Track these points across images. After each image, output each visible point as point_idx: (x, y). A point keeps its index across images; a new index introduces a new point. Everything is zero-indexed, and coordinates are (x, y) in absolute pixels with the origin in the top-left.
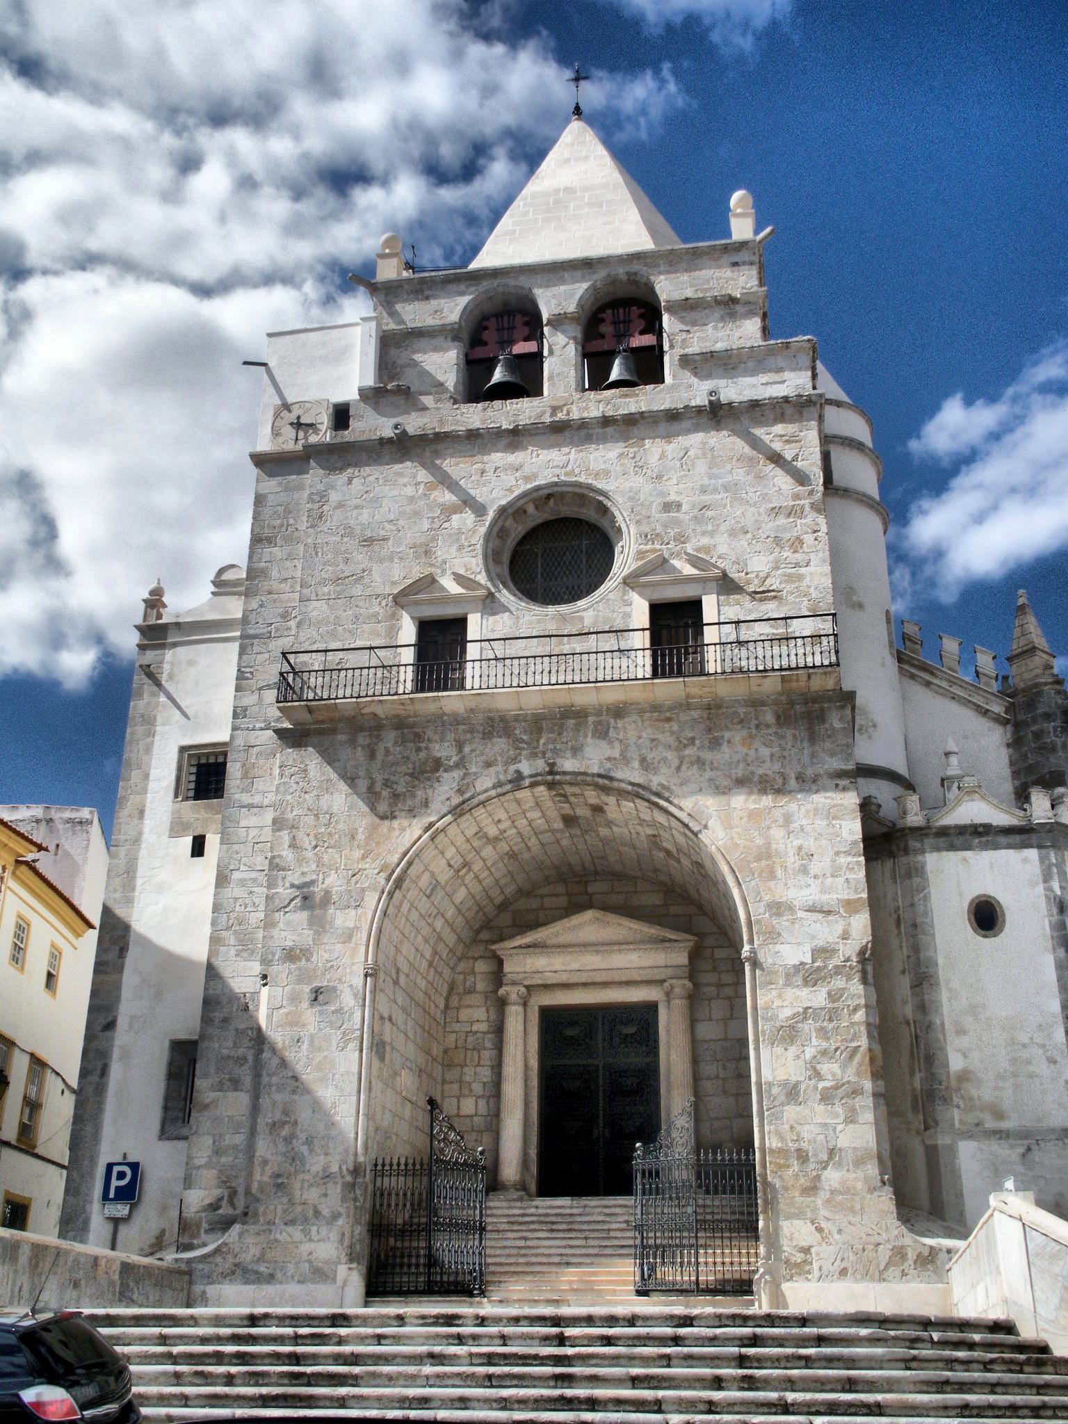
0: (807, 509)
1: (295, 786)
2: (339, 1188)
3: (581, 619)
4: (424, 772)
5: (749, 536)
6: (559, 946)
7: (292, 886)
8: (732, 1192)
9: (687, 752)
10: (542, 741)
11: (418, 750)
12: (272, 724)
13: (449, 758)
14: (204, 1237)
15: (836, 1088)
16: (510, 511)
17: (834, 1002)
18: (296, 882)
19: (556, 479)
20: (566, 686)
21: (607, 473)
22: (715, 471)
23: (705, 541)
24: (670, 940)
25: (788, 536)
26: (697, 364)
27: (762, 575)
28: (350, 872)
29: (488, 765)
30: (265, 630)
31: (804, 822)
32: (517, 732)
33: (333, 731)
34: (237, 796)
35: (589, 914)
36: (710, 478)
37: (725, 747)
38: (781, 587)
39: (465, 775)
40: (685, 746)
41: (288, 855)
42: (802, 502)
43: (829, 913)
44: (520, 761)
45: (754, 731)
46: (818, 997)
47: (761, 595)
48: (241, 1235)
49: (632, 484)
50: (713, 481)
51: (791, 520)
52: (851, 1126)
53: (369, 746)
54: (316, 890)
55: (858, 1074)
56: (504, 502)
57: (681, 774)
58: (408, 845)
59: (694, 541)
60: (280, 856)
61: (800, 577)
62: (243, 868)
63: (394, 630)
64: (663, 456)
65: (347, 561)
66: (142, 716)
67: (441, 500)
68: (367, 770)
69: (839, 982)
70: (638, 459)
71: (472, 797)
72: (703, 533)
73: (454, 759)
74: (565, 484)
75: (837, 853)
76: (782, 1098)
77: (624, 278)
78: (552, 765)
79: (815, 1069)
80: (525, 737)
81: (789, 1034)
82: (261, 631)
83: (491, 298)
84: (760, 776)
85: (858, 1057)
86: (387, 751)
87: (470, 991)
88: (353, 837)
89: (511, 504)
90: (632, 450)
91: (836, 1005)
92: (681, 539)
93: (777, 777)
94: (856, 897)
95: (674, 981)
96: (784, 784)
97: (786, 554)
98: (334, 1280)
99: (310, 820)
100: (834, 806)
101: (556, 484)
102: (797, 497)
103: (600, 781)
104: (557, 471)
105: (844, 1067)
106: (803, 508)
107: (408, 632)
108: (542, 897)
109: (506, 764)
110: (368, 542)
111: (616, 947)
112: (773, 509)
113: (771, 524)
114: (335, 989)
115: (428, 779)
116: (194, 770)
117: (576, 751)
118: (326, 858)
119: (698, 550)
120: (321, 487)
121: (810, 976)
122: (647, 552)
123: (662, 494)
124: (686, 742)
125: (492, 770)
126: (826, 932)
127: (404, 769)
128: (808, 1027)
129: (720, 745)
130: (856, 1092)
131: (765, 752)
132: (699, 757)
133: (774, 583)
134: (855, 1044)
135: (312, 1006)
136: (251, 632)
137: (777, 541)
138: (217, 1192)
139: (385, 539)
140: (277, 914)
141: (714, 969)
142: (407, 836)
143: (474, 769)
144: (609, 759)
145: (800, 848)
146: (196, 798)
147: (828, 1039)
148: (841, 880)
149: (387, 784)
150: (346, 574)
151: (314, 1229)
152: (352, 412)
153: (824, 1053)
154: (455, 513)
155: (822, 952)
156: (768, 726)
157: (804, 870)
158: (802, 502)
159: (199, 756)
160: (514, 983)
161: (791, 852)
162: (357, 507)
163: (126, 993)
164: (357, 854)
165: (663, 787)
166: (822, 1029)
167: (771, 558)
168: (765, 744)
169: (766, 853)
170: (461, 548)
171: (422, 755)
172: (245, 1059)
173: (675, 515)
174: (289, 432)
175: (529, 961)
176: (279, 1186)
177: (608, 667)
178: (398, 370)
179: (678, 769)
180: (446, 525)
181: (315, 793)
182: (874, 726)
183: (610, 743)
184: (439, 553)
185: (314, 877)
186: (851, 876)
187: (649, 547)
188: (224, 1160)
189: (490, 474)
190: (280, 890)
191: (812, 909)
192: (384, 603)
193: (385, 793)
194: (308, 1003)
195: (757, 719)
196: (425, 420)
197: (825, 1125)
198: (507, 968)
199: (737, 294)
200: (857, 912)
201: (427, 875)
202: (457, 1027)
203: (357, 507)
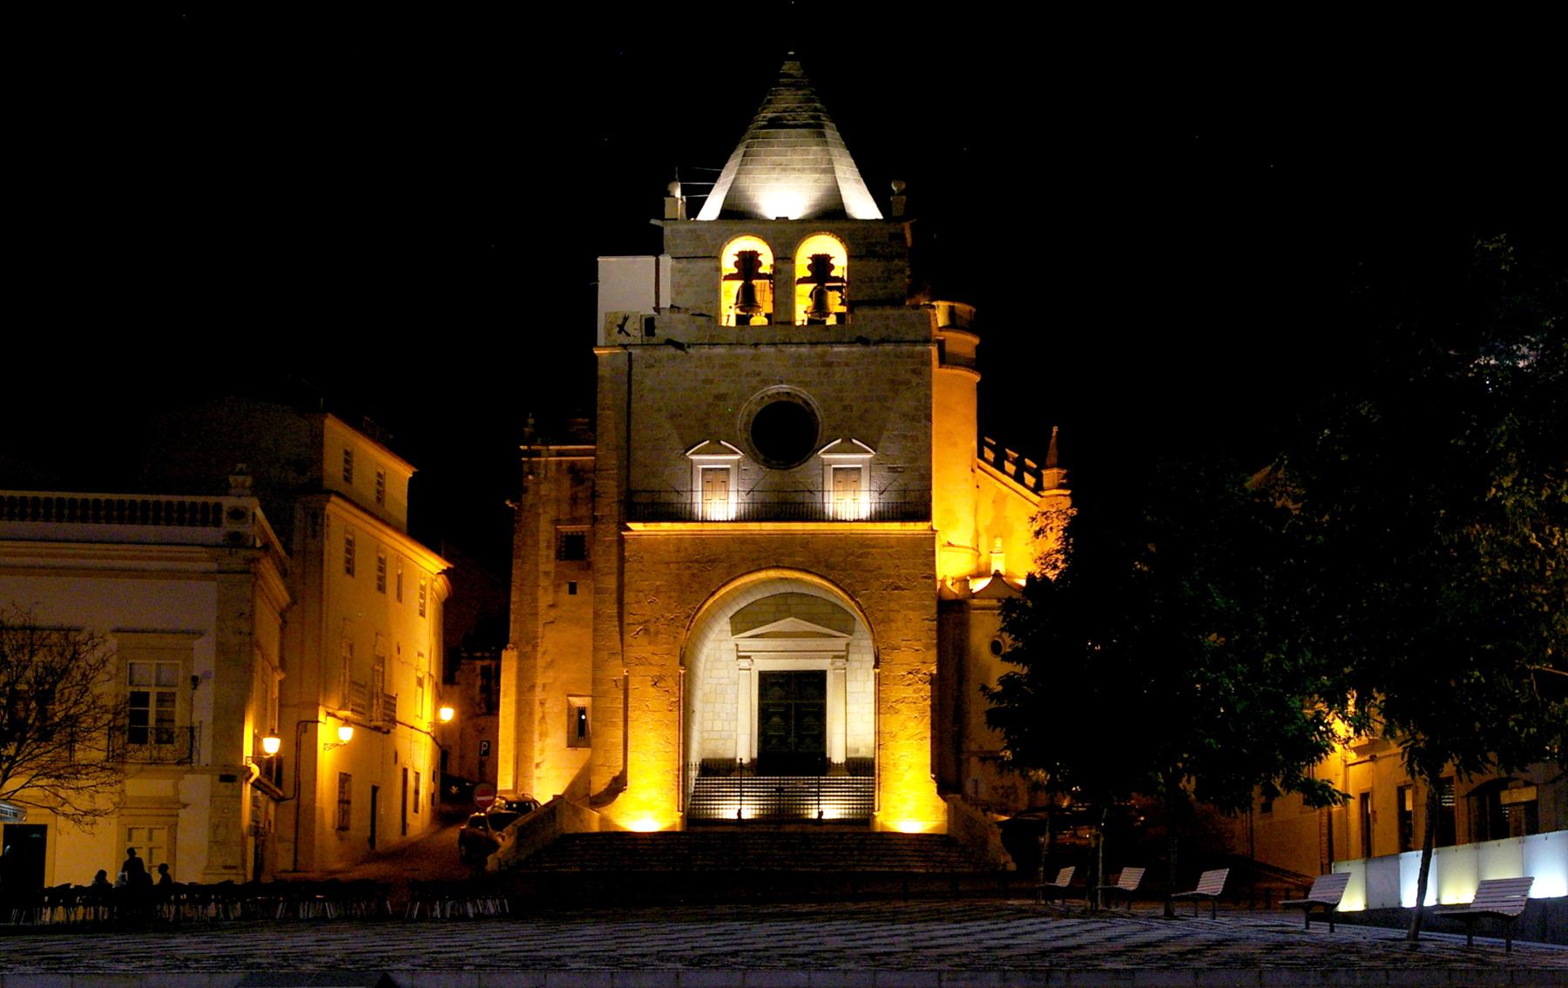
24: (835, 637)
87: (719, 660)
102: (917, 409)
105: (917, 725)
135: (653, 686)
163: (540, 670)
202: (710, 680)
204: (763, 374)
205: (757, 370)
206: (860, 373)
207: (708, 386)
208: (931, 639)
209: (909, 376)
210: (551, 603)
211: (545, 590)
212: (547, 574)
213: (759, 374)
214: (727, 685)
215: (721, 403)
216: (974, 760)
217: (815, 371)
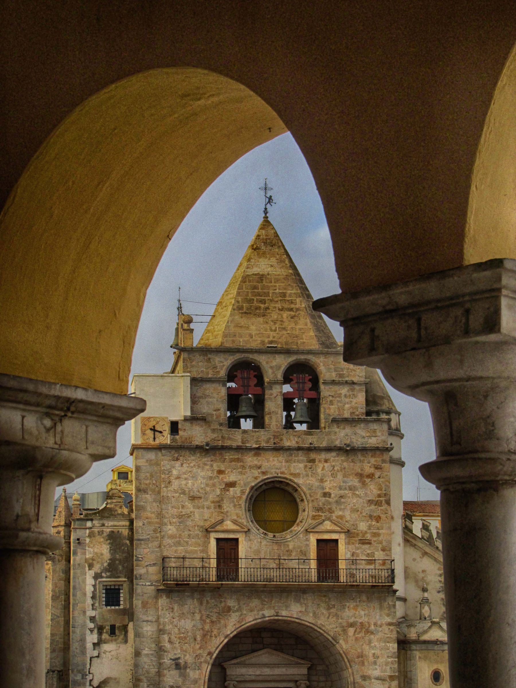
0: (383, 502)
1: (168, 615)
3: (288, 546)
4: (224, 612)
5: (359, 513)
6: (252, 664)
7: (171, 659)
9: (332, 610)
10: (273, 602)
11: (221, 602)
12: (154, 584)
13: (234, 607)
16: (255, 488)
18: (172, 658)
19: (276, 475)
20: (287, 583)
22: (345, 479)
23: (341, 513)
25: (375, 515)
27: (363, 531)
28: (195, 655)
29: (251, 611)
30: (147, 537)
31: (376, 643)
32: (263, 597)
34: (141, 616)
35: (265, 650)
36: (344, 482)
37: (347, 610)
38: (371, 539)
39: (241, 615)
40: (331, 608)
41: (168, 645)
42: (381, 499)
43: (384, 680)
44: (264, 610)
45: (358, 603)
47: (364, 542)
49: (310, 482)
50: (344, 484)
51: (376, 507)
53: (199, 599)
54: (181, 661)
56: (253, 484)
57: (329, 620)
58: (218, 644)
59: (336, 513)
60: (164, 646)
61: (378, 535)
62: (146, 649)
63: (206, 543)
64: (323, 469)
65: (183, 507)
66: (79, 564)
67: (225, 480)
68: (199, 609)
70: (312, 469)
72: (340, 509)
73: (236, 607)
74: (280, 477)
75: (388, 657)
78: (278, 612)
82: (144, 537)
84: (361, 623)
88: (195, 639)
89: (256, 485)
90: (310, 464)
93: (366, 624)
95: (302, 681)
96: (369, 627)
99: (176, 630)
100: (388, 637)
101: (276, 477)
102: (379, 496)
103: (297, 621)
104: (277, 471)
106: (381, 501)
109: (259, 610)
110: (193, 498)
112: (369, 501)
113: (368, 508)
115: (226, 615)
116: (104, 591)
117: (287, 607)
118: (184, 648)
119: (337, 517)
120: (168, 467)
122: (316, 516)
123: (323, 488)
124: (331, 606)
125: (253, 614)
127: (215, 610)
129: (344, 608)
131: (362, 613)
132: (336, 613)
133: (368, 536)
136: (141, 538)
137: (371, 516)
139: (200, 498)
140: (165, 671)
141: (316, 675)
142: (218, 639)
143: (245, 612)
144: (300, 612)
145: (374, 654)
146: (106, 605)
148: (388, 668)
149: (208, 616)
150: (184, 513)
152: (180, 426)
154: (231, 487)
157: (375, 663)
158: (381, 499)
159: (106, 585)
161: (371, 655)
162: (186, 479)
164: (198, 647)
165: (323, 625)
167: (367, 524)
168: (362, 610)
169: (361, 656)
170: (235, 506)
171: (223, 604)
173: (327, 499)
174: (150, 433)
175: (238, 670)
178: (197, 399)
179: (328, 618)
180: (228, 493)
181: (177, 618)
183: (301, 604)
184: (225, 507)
185: (179, 656)
186: (393, 666)
187: (317, 514)
189: (248, 470)
190: (166, 661)
191: (377, 679)
192: (201, 530)
193: (208, 621)
196: (215, 435)
198: (228, 672)
199: (355, 380)
200: (394, 680)
203: (186, 479)
205: (259, 464)
206: (336, 468)
207: (221, 476)
208: (394, 672)
209: (372, 470)
210: (96, 641)
211: (91, 631)
212: (92, 619)
213: (260, 467)
215: (231, 489)
217: (301, 465)
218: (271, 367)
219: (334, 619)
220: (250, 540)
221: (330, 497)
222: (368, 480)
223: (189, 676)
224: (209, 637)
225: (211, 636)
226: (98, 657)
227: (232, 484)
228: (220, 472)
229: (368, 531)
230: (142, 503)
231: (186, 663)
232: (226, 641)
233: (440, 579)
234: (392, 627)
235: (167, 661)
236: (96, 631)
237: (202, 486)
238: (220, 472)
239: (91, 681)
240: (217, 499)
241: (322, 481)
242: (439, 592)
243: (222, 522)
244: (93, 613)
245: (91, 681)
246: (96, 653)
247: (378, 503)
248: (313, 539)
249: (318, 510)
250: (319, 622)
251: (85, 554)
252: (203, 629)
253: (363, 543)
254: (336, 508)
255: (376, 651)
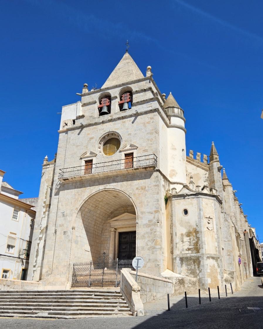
0: (154, 132)
2: (66, 268)
7: (61, 213)
8: (100, 268)
14: (45, 277)
15: (150, 247)
16: (101, 138)
17: (151, 230)
18: (62, 212)
21: (118, 128)
23: (135, 141)
26: (139, 103)
33: (69, 184)
43: (152, 213)
46: (148, 230)
48: (50, 277)
52: (153, 254)
55: (155, 244)
56: (100, 136)
69: (153, 227)
71: (92, 194)
74: (111, 132)
75: (154, 201)
76: (141, 249)
77: (126, 88)
79: (147, 244)
80: (101, 182)
81: (143, 237)
83: (102, 95)
85: (155, 241)
86: (78, 186)
88: (71, 203)
91: (151, 231)
92: (131, 141)
94: (157, 210)
97: (149, 142)
98: (65, 285)
99: (65, 200)
100: (154, 192)
101: (109, 132)
102: (152, 130)
105: (152, 243)
107: (83, 163)
108: (119, 211)
111: (130, 220)
112: (148, 133)
114: (67, 232)
121: (148, 226)
126: (151, 217)
128: (146, 235)
130: (154, 248)
133: (147, 148)
134: (154, 239)
135: (64, 235)
136: (58, 165)
137: (148, 140)
138: (48, 269)
147: (149, 238)
148: (154, 207)
151: (62, 275)
153: (149, 240)
155: (150, 221)
156: (143, 177)
160: (112, 228)
162: (75, 140)
165: (124, 190)
166: (149, 236)
169: (141, 202)
172: (53, 245)
176: (57, 268)
177: (118, 167)
179: (127, 187)
180: (90, 142)
182: (177, 173)
188: (49, 263)
194: (63, 233)
195: (141, 176)
197: (148, 255)
199: (145, 89)
201: (86, 209)
202: (103, 236)
204: (104, 129)
207: (89, 136)
209: (149, 120)
211: (44, 207)
214: (108, 237)
215: (92, 140)
216: (178, 259)
217: (120, 125)
218: (113, 93)
219: (129, 187)
220: (97, 158)
221: (131, 135)
222: (147, 125)
223: (67, 219)
224: (77, 201)
225: (78, 201)
226: (44, 217)
227: (92, 138)
228: (88, 134)
229: (147, 146)
230: (60, 152)
231: (67, 214)
232: (83, 202)
233: (205, 176)
234: (156, 187)
235: (60, 214)
236: (45, 207)
237: (81, 141)
238: (88, 134)
239: (41, 227)
240: (86, 145)
241: (127, 129)
242: (205, 182)
243: (86, 153)
244: (45, 200)
245: (41, 227)
246: (44, 216)
247: (151, 133)
248: (123, 154)
249: (125, 141)
250: (122, 189)
251: (45, 178)
252: (75, 198)
253: (144, 152)
254: (133, 139)
255: (148, 200)
